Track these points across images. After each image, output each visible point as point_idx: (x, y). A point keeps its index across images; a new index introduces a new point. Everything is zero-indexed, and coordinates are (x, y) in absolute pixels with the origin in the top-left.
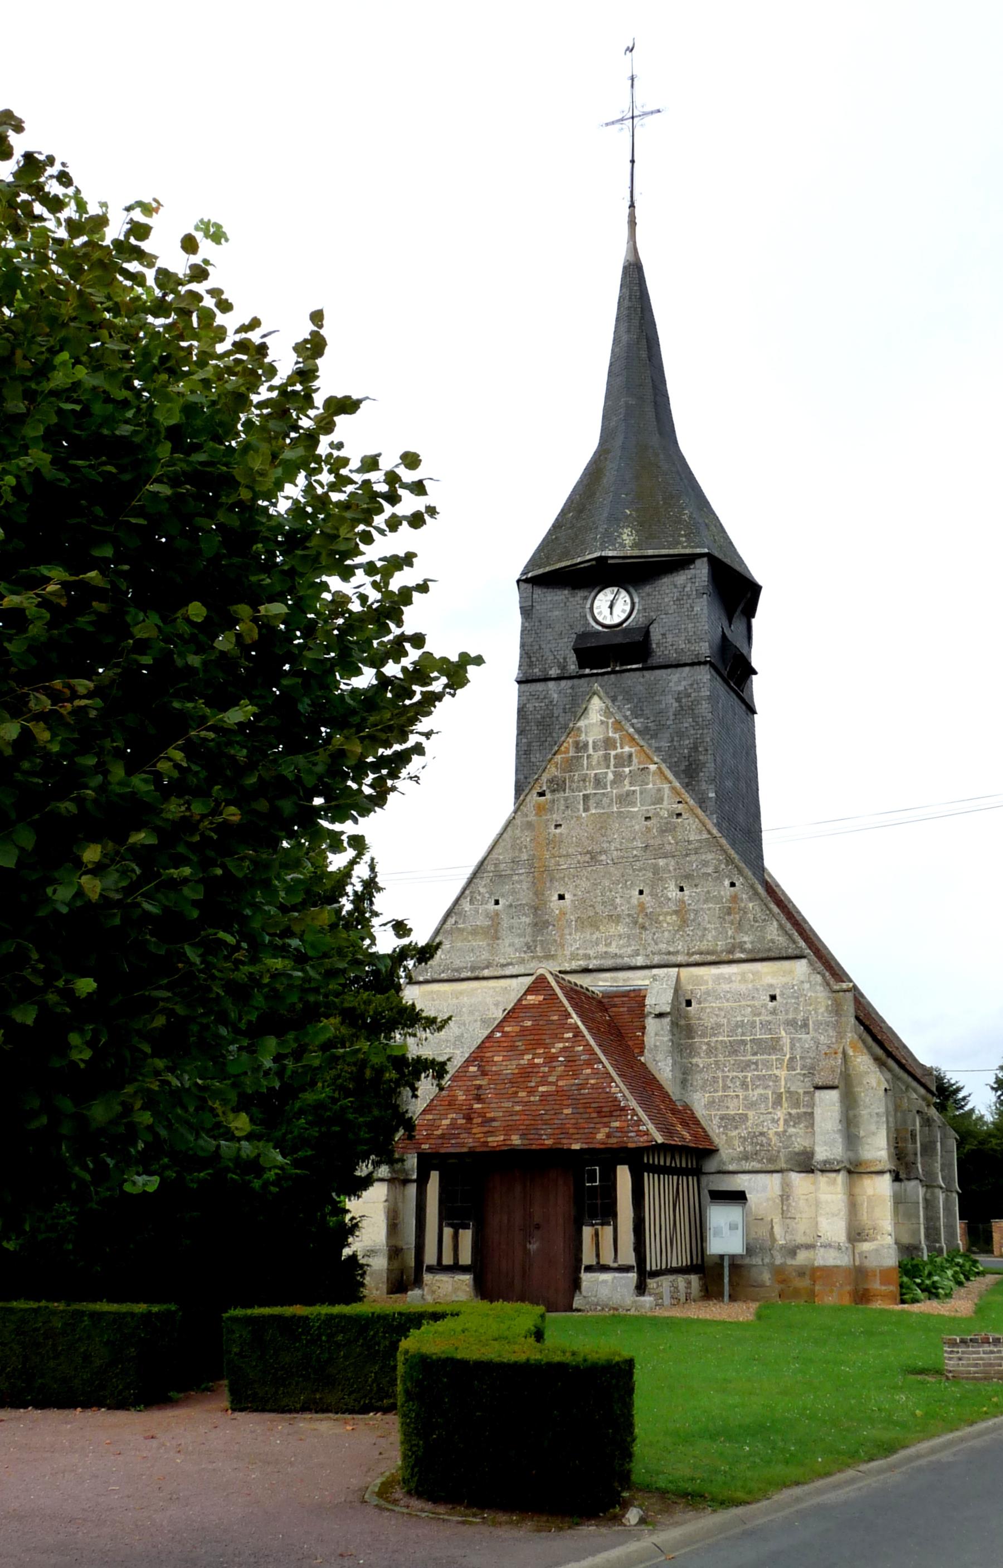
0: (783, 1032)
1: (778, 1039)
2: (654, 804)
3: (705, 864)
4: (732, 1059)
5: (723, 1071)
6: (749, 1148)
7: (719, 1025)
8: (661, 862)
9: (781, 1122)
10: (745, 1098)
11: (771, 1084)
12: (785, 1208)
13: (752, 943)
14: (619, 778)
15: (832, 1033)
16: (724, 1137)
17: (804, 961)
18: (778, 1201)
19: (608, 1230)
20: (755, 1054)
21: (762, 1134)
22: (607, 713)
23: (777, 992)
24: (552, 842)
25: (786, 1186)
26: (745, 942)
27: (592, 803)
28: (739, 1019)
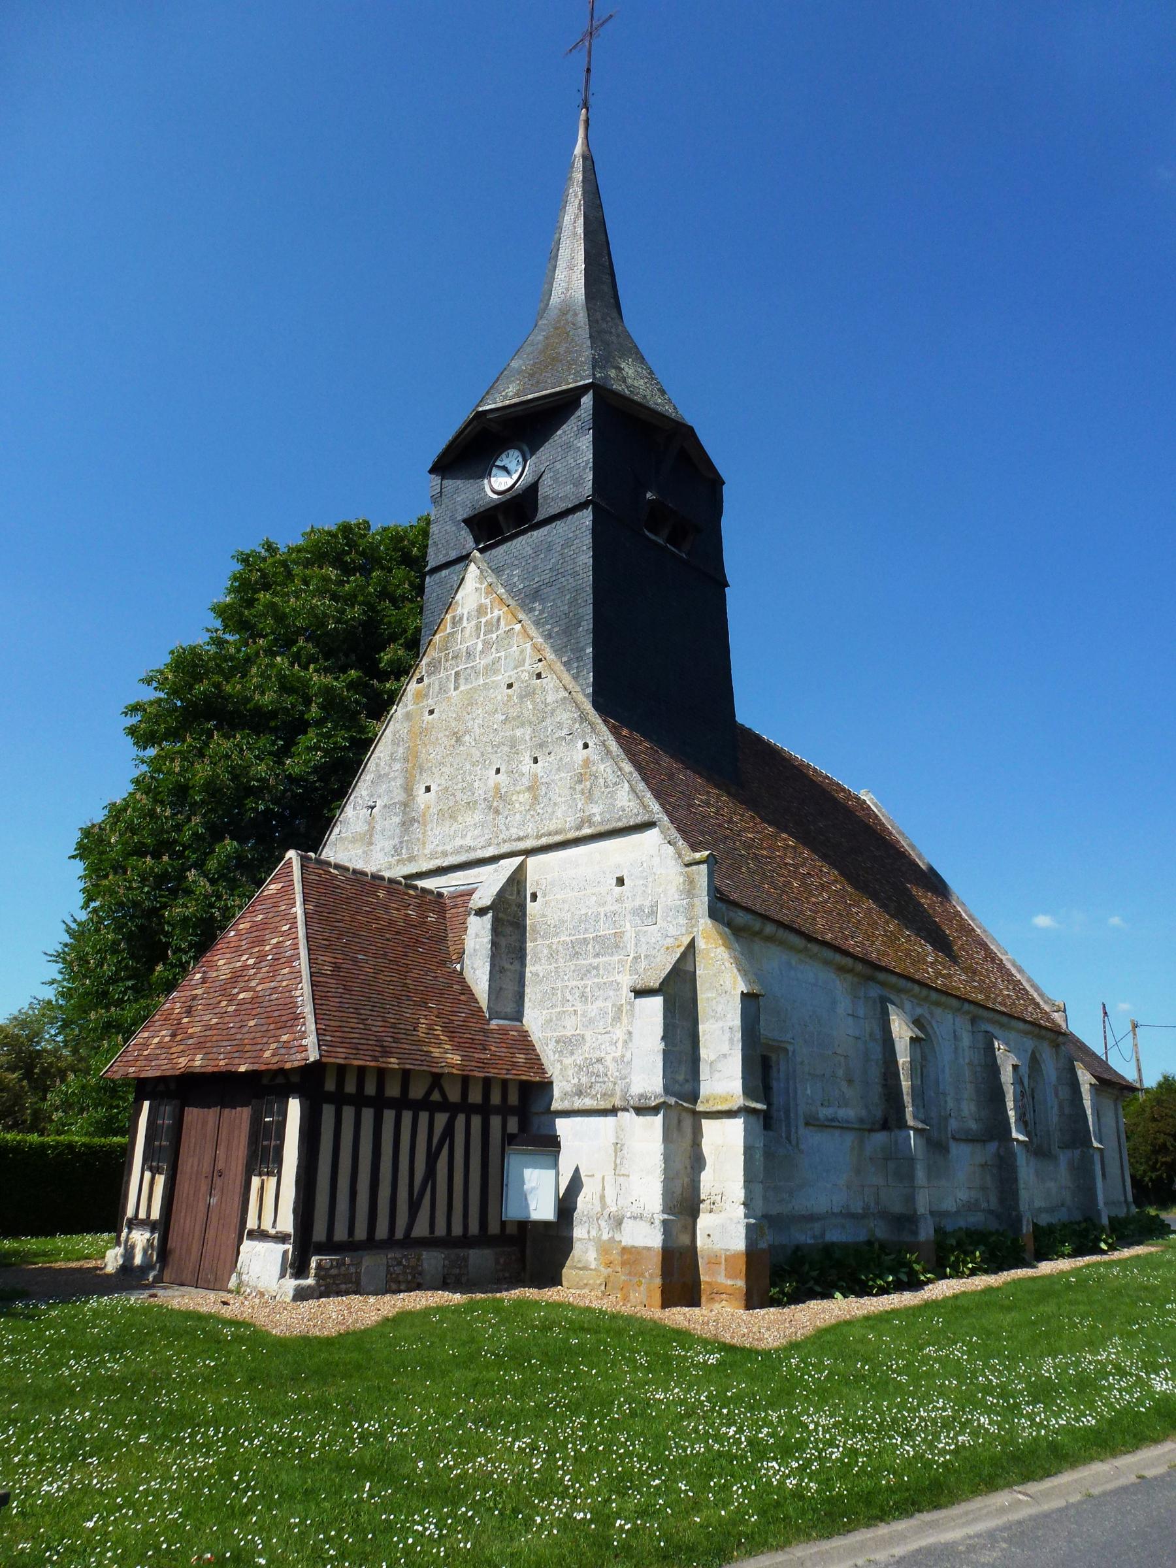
0: (628, 924)
1: (619, 935)
2: (516, 668)
3: (560, 726)
4: (571, 965)
5: (563, 980)
6: (584, 1080)
7: (563, 922)
8: (519, 733)
9: (620, 1044)
10: (583, 1015)
11: (611, 993)
12: (618, 1162)
13: (602, 813)
14: (487, 645)
15: (682, 920)
16: (558, 1066)
17: (655, 832)
18: (611, 1150)
19: (273, 1180)
20: (597, 955)
21: (599, 1060)
22: (482, 577)
23: (625, 874)
24: (425, 731)
25: (619, 1129)
26: (594, 814)
27: (462, 680)
28: (583, 912)
